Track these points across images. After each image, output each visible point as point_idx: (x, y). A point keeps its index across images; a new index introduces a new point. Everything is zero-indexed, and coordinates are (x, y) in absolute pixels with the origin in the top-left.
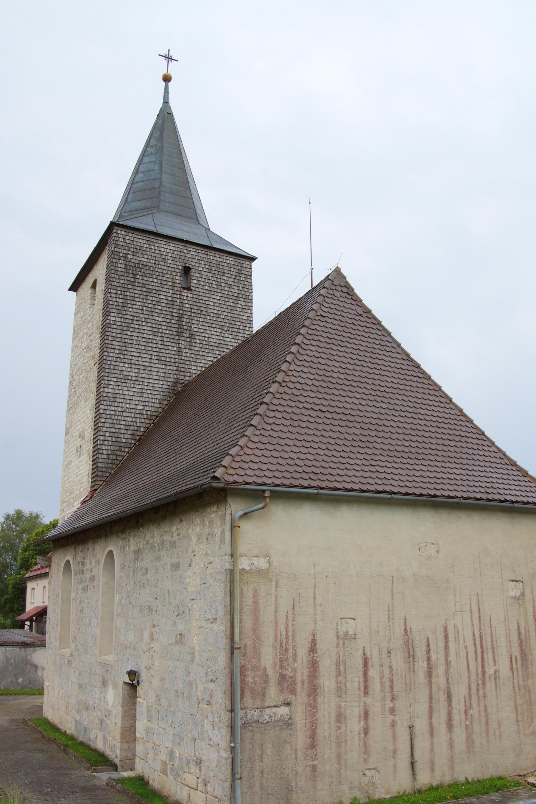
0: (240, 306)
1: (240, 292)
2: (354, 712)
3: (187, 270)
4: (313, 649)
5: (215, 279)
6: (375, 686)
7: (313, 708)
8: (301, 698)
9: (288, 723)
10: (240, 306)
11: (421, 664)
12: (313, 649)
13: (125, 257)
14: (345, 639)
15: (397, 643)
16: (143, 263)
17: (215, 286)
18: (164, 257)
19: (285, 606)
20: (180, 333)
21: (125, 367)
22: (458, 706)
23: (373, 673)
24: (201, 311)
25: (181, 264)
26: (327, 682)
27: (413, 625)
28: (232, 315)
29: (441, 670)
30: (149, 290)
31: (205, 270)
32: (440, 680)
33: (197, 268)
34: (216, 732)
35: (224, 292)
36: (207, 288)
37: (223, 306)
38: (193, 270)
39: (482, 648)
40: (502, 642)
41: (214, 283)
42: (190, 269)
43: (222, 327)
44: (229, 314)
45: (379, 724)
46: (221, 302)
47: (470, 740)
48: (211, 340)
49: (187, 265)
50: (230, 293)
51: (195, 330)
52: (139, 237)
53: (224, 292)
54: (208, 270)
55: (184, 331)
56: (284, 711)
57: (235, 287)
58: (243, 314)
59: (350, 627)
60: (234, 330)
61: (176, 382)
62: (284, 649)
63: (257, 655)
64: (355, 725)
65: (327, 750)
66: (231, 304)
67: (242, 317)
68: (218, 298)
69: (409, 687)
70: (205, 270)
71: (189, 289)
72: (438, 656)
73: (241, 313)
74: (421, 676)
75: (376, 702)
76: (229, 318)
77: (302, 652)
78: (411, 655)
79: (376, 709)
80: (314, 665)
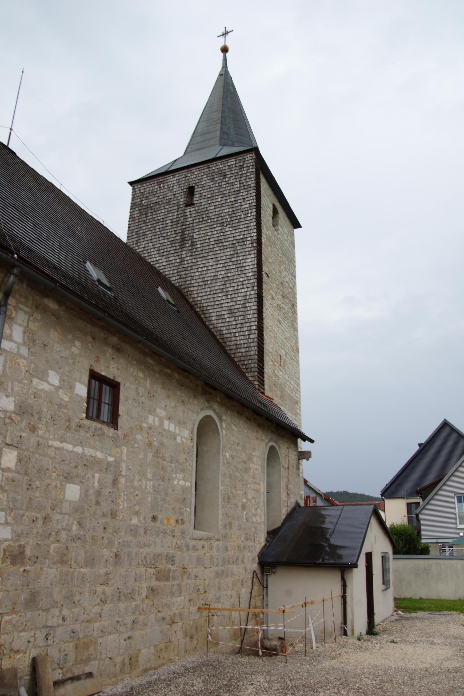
0: (241, 198)
1: (242, 185)
5: (217, 185)
10: (241, 198)
13: (140, 204)
16: (153, 202)
17: (216, 191)
18: (171, 189)
20: (182, 247)
24: (203, 218)
25: (185, 187)
28: (233, 209)
30: (157, 221)
31: (207, 181)
33: (200, 183)
35: (225, 192)
36: (209, 196)
37: (224, 205)
38: (196, 187)
41: (215, 188)
42: (194, 187)
43: (222, 224)
44: (231, 210)
46: (222, 202)
48: (212, 240)
49: (191, 185)
50: (232, 190)
51: (197, 237)
52: (151, 183)
53: (225, 192)
54: (210, 181)
55: (186, 242)
57: (236, 183)
58: (245, 203)
60: (234, 222)
66: (233, 199)
67: (244, 207)
68: (219, 200)
70: (207, 181)
73: (243, 203)
76: (230, 213)
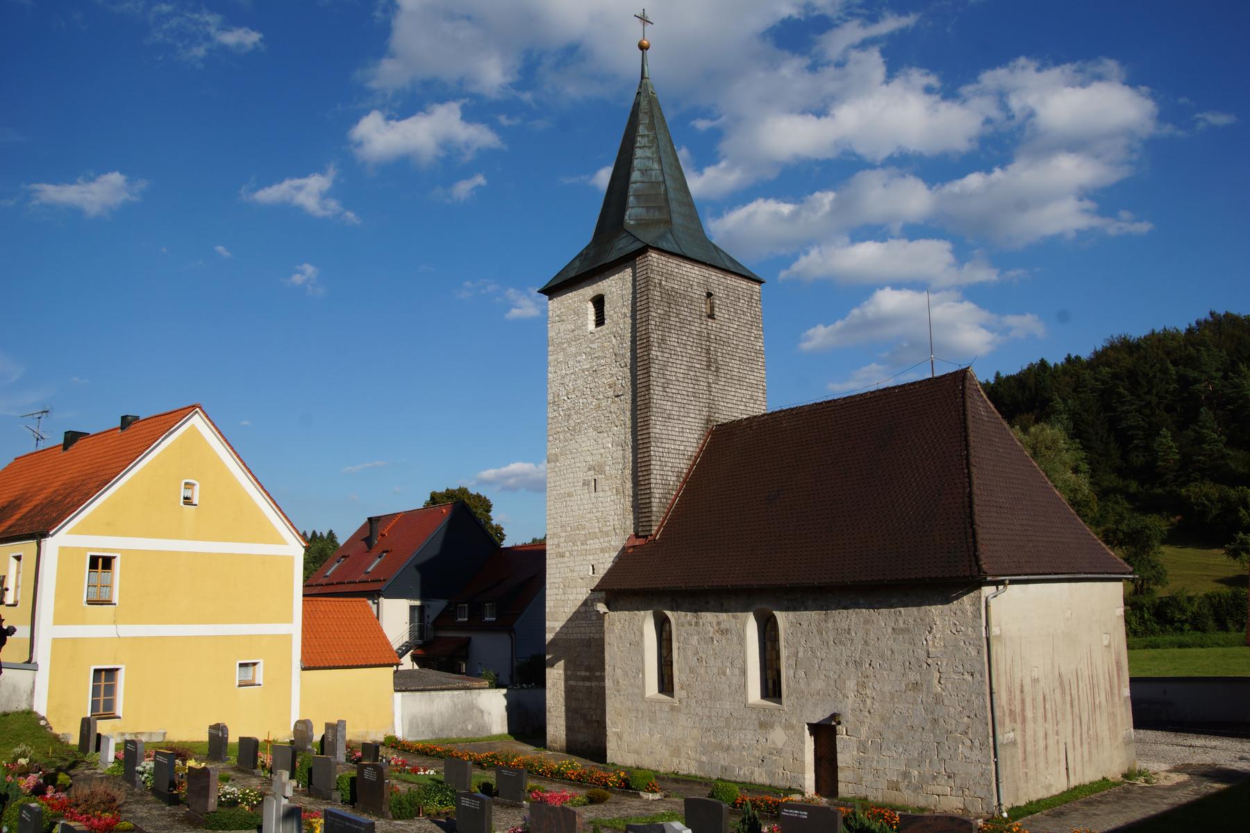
2: (1041, 734)
3: (709, 295)
4: (1022, 691)
6: (1049, 715)
7: (1024, 731)
8: (1018, 726)
9: (1014, 743)
11: (1068, 698)
12: (1022, 691)
14: (1035, 681)
15: (1057, 684)
19: (1009, 661)
21: (668, 405)
22: (1085, 728)
23: (1048, 706)
26: (1029, 714)
27: (1063, 671)
29: (1076, 703)
32: (1076, 710)
34: (977, 752)
39: (1093, 687)
40: (1102, 681)
45: (1051, 742)
47: (1090, 752)
56: (1011, 735)
59: (1035, 675)
61: (708, 421)
62: (1010, 692)
63: (1000, 697)
64: (1042, 743)
65: (1031, 762)
69: (1064, 714)
71: (711, 316)
72: (1074, 692)
74: (1068, 706)
75: (1049, 726)
77: (1018, 692)
78: (1063, 693)
79: (1050, 732)
80: (1023, 702)
